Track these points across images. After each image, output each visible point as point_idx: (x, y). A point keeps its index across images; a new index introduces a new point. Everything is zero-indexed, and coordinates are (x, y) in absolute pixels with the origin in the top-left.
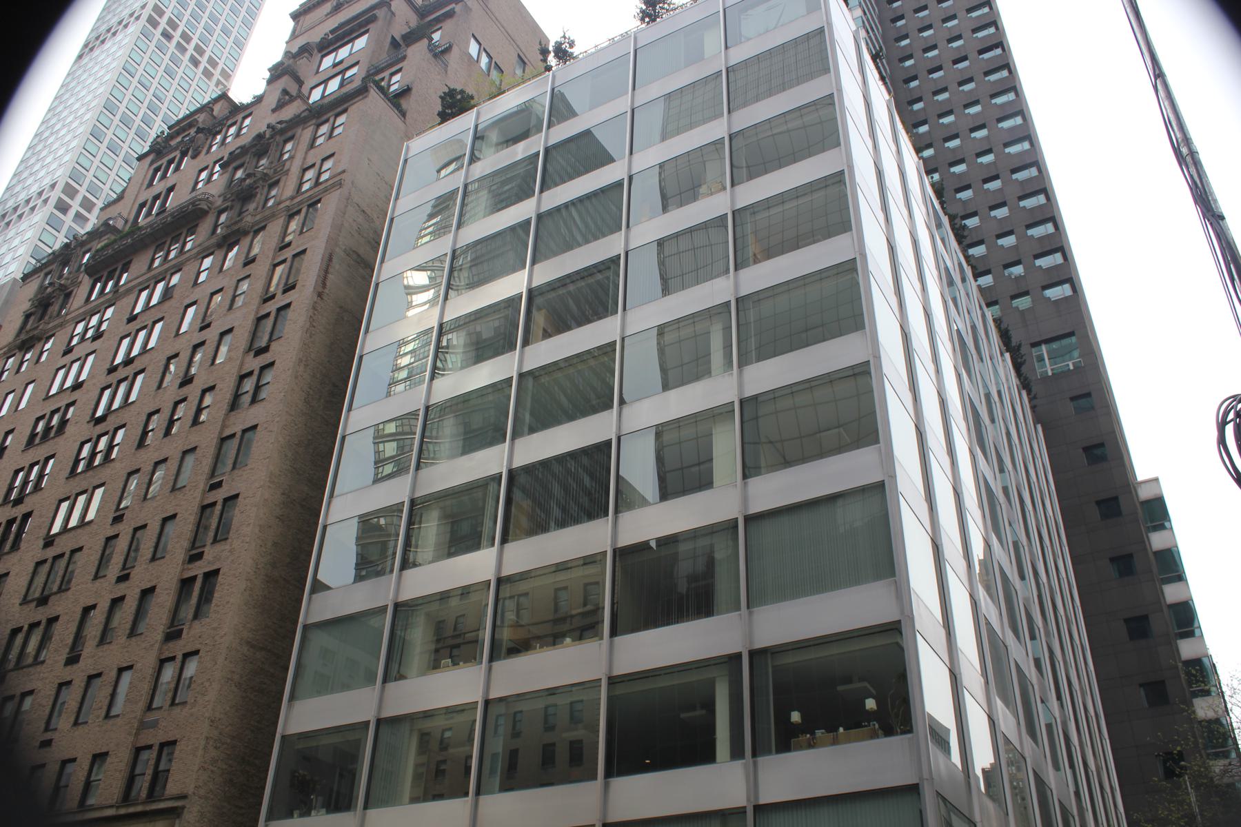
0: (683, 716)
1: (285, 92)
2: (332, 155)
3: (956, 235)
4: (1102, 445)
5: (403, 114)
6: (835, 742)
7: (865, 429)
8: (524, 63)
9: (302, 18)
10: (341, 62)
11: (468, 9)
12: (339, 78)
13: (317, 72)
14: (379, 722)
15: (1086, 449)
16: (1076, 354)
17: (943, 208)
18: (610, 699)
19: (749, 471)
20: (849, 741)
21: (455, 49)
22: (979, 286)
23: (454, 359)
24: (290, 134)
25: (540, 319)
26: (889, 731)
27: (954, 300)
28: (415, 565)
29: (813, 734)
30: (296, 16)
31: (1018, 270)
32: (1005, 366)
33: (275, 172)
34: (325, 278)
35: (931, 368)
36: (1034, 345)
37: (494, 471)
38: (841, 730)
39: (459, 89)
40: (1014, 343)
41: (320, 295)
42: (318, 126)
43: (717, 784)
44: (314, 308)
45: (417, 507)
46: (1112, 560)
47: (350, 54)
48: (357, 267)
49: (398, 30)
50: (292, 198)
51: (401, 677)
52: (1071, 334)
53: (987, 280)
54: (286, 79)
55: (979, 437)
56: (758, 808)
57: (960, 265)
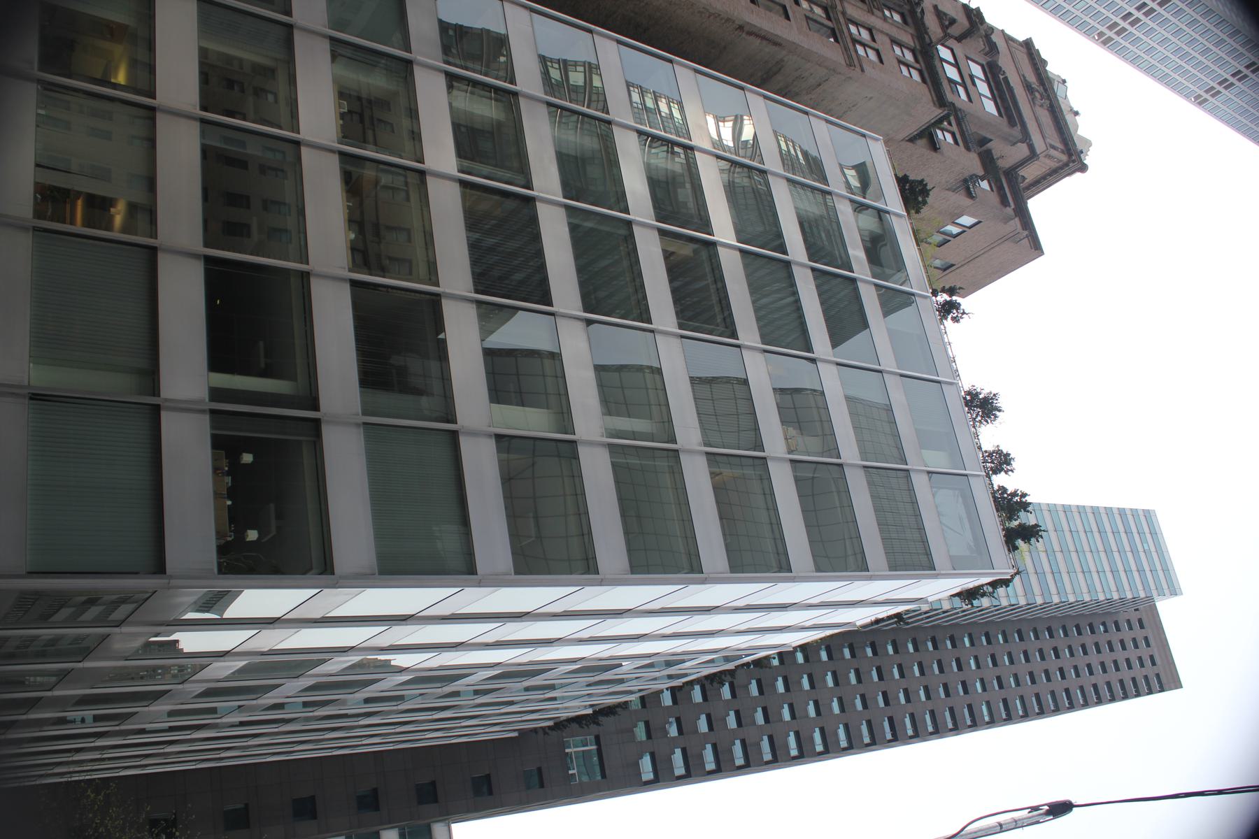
0: (261, 344)
2: (881, 61)
3: (715, 674)
4: (490, 793)
5: (912, 140)
6: (217, 495)
7: (531, 562)
9: (1024, 50)
10: (974, 84)
11: (1007, 220)
12: (958, 79)
13: (968, 58)
14: (290, 27)
15: (488, 777)
16: (585, 779)
17: (743, 665)
18: (286, 272)
20: (216, 509)
21: (968, 202)
22: (662, 691)
23: (660, 158)
24: (909, 20)
25: (686, 250)
26: (222, 550)
27: (651, 665)
28: (450, 87)
29: (228, 473)
30: (1028, 44)
31: (673, 731)
32: (579, 707)
34: (757, 36)
35: (585, 635)
36: (598, 740)
37: (536, 182)
38: (229, 503)
39: (929, 200)
40: (602, 719)
41: (741, 28)
42: (913, 51)
43: (186, 370)
44: (728, 20)
45: (509, 98)
46: (375, 791)
47: (980, 95)
49: (997, 147)
50: (844, 13)
51: (334, 56)
52: (604, 776)
53: (667, 700)
55: (511, 674)
56: (156, 409)
57: (686, 675)
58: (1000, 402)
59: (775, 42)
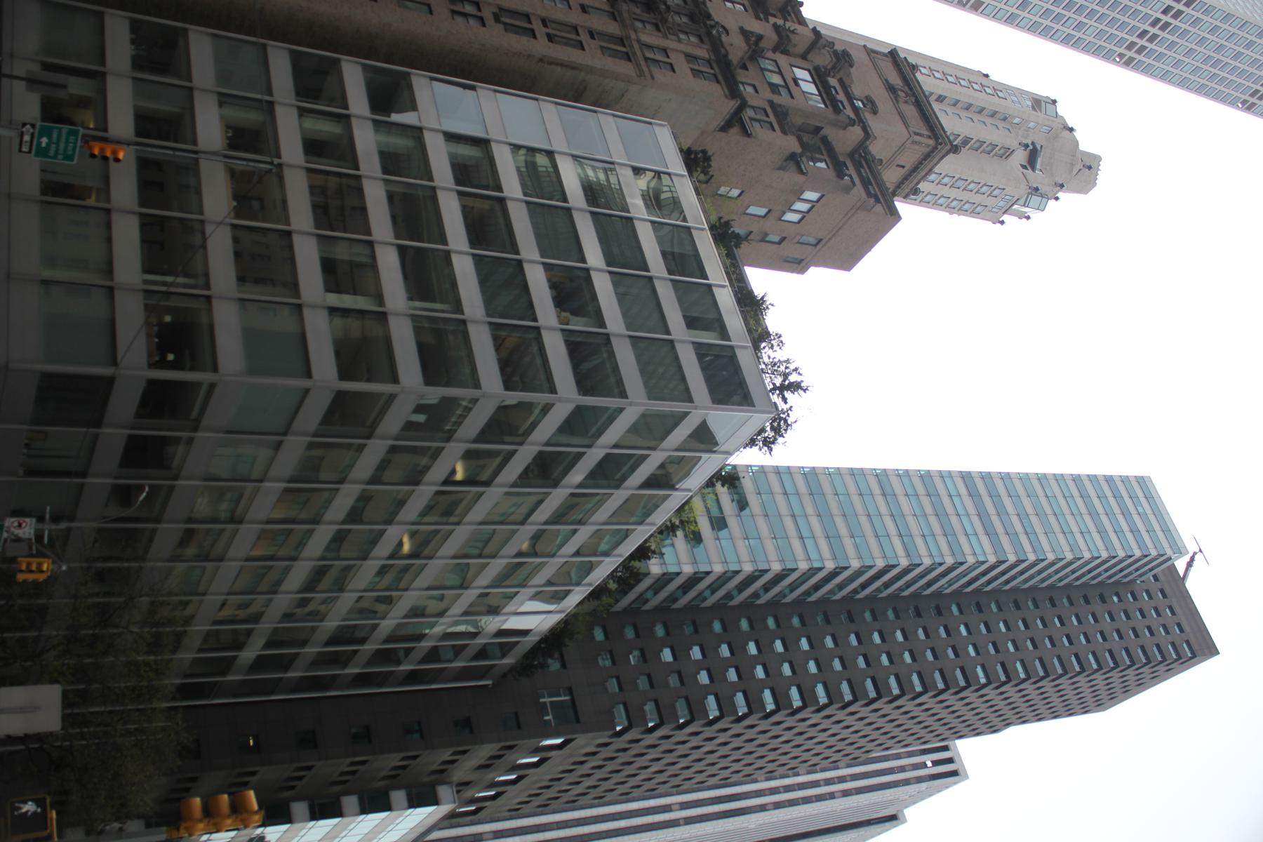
1: (760, 38)
5: (725, 128)
8: (816, 245)
11: (847, 190)
21: (800, 179)
28: (300, 116)
33: (669, 28)
37: (362, 166)
39: (712, 163)
48: (576, 91)
50: (638, 41)
54: (775, 37)
58: (769, 300)
59: (573, 67)
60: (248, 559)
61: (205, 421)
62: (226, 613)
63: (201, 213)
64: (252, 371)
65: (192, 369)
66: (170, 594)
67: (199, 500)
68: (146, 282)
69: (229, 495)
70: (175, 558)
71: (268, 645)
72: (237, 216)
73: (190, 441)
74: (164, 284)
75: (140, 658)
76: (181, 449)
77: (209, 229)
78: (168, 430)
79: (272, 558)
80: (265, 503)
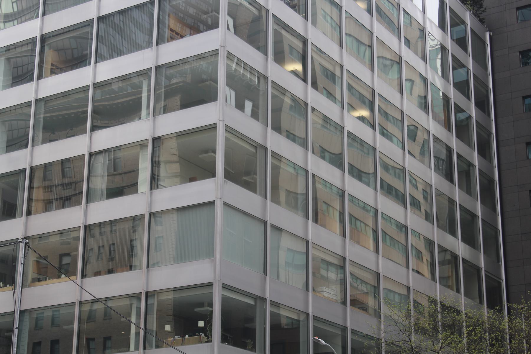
19: (155, 182)
25: (50, 56)
29: (174, 337)
38: (187, 336)
60: (377, 251)
61: (258, 293)
62: (425, 270)
63: (73, 304)
64: (210, 253)
65: (211, 305)
66: (408, 316)
67: (326, 295)
68: (137, 348)
69: (323, 272)
70: (377, 314)
71: (453, 232)
72: (75, 274)
73: (274, 304)
74: (137, 334)
75: (465, 340)
76: (283, 313)
77: (87, 297)
78: (265, 323)
79: (375, 232)
80: (326, 238)
